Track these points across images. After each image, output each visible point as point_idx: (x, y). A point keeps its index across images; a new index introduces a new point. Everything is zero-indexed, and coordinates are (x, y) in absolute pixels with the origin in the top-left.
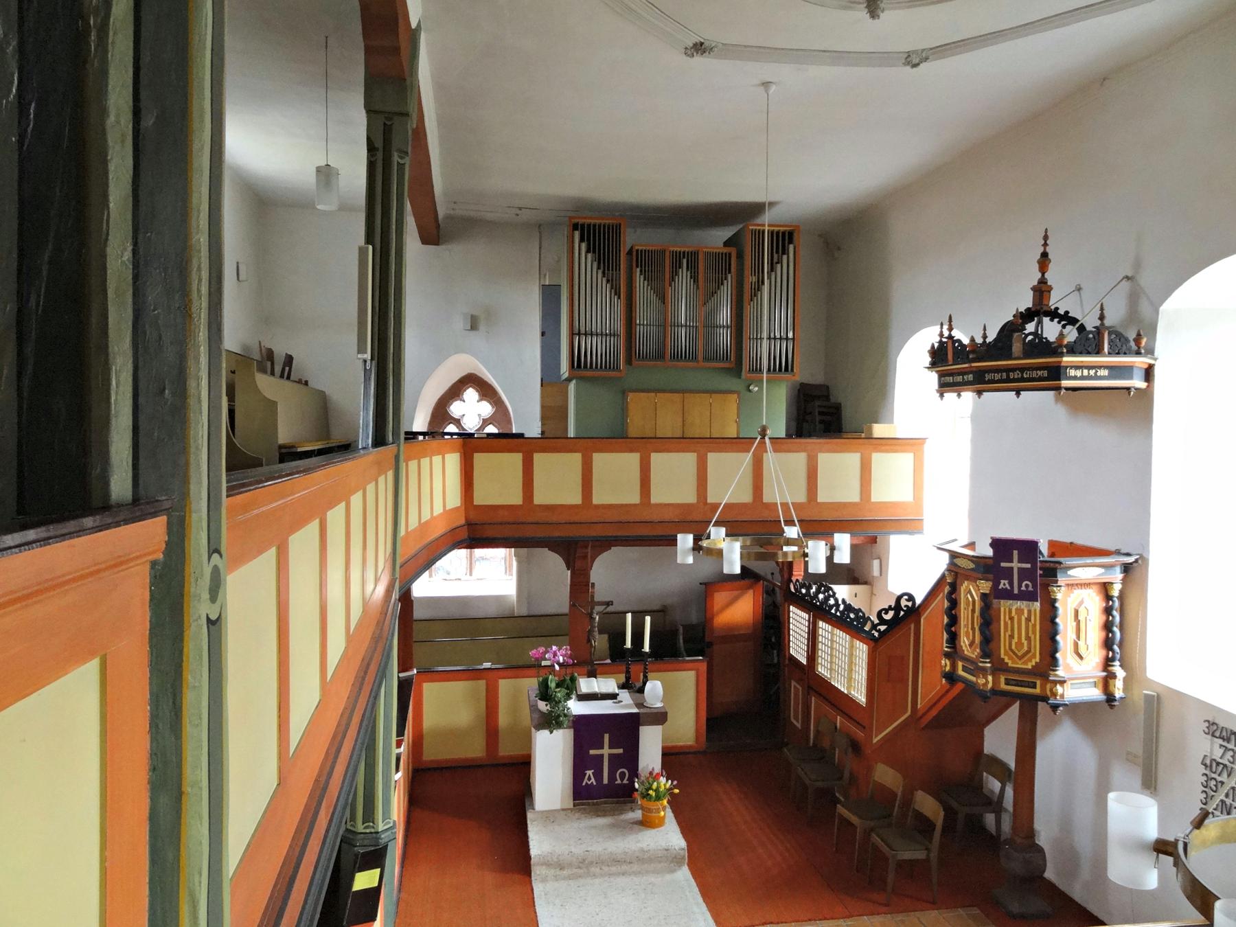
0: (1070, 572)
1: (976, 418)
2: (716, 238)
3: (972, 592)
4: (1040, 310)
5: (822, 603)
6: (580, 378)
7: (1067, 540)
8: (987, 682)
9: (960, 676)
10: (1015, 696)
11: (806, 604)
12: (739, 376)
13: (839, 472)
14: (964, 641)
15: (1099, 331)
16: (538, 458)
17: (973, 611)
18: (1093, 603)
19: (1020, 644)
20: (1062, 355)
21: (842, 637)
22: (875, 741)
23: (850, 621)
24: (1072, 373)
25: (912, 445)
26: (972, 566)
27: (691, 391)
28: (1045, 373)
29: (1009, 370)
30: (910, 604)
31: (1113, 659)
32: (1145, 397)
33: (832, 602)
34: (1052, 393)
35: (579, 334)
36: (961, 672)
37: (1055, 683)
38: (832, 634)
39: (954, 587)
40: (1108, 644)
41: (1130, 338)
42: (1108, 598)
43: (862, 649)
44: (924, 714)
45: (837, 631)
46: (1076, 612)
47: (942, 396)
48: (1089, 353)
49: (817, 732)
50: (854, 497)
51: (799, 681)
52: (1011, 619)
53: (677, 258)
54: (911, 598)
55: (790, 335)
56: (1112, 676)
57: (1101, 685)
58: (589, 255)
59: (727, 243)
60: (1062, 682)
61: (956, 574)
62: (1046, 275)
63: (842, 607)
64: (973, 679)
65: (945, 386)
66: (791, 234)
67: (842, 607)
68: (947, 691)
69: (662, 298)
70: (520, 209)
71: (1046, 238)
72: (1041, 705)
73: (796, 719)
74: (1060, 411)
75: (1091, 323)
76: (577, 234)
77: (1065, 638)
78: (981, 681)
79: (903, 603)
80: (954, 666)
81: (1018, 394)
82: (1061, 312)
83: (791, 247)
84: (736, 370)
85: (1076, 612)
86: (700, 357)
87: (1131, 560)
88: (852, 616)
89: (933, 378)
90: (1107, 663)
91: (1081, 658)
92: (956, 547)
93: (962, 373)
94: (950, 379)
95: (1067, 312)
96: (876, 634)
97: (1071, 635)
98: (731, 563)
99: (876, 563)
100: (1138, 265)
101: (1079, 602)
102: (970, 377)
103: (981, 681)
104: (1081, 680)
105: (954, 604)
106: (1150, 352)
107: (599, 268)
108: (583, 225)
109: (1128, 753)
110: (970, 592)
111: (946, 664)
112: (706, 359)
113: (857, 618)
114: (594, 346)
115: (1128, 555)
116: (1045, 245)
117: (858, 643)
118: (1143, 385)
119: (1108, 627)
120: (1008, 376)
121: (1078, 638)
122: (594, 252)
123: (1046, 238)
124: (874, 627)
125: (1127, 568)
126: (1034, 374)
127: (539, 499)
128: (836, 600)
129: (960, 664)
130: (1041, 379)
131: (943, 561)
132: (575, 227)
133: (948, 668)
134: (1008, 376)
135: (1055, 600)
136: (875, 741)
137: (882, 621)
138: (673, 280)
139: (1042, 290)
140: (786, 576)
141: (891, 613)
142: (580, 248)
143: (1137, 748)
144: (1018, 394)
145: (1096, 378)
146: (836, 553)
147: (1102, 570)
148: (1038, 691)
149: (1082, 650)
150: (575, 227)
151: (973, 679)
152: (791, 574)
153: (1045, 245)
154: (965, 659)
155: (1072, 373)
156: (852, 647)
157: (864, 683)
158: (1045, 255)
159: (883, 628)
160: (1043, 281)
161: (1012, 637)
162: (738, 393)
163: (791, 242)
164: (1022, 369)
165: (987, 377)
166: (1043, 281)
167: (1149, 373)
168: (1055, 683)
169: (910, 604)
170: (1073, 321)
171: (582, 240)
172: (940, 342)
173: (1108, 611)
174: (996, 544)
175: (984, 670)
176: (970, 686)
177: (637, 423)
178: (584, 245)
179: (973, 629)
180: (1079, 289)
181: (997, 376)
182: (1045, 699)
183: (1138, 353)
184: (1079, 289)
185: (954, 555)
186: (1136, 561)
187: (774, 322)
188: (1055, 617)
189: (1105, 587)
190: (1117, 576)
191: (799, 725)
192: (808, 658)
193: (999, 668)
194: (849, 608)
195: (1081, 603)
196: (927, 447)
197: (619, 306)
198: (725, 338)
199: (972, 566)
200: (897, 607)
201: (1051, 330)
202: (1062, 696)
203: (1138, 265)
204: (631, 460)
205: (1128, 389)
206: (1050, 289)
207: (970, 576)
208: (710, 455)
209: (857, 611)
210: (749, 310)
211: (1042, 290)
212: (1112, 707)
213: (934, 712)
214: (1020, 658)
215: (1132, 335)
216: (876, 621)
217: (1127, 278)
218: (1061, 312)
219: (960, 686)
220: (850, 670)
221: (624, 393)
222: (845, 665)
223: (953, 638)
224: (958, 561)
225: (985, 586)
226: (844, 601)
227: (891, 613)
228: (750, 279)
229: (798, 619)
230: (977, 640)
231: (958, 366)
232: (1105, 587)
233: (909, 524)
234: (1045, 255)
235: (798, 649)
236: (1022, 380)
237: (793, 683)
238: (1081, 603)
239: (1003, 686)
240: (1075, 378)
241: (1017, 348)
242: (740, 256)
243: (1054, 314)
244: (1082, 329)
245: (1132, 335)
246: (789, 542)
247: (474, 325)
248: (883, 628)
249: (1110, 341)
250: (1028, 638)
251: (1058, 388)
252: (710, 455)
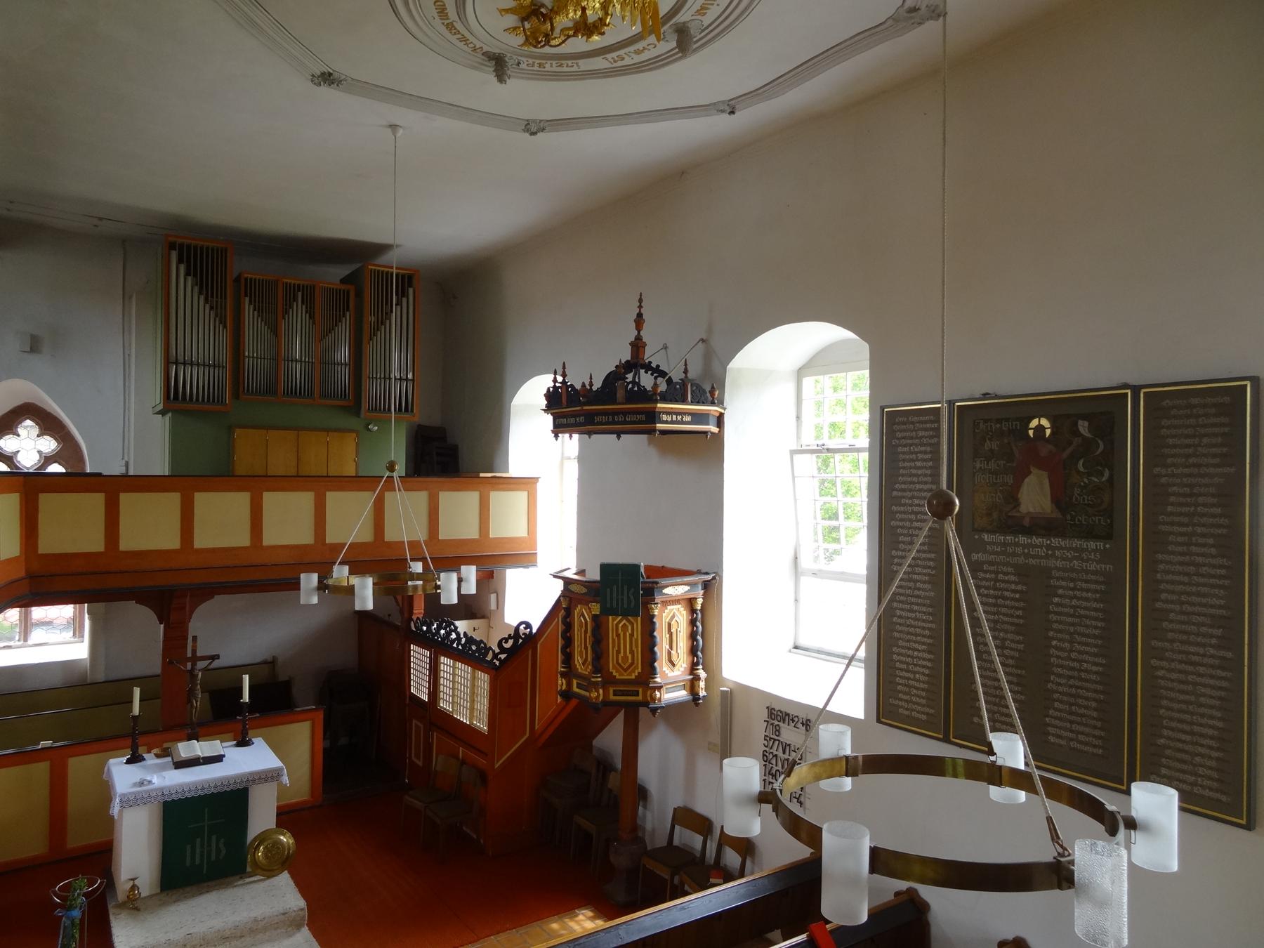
0: (666, 591)
1: (582, 459)
2: (334, 274)
3: (584, 615)
4: (636, 362)
5: (443, 639)
6: (176, 412)
7: (659, 564)
8: (597, 695)
9: (576, 693)
10: (619, 705)
11: (426, 641)
12: (357, 413)
13: (458, 512)
14: (578, 660)
15: (684, 383)
16: (125, 498)
17: (586, 632)
18: (679, 616)
19: (625, 657)
20: (656, 402)
21: (464, 669)
23: (472, 654)
24: (664, 417)
25: (527, 484)
26: (584, 590)
27: (303, 429)
28: (643, 417)
29: (615, 413)
31: (697, 664)
32: (718, 439)
33: (454, 636)
34: (645, 437)
35: (176, 363)
36: (575, 689)
37: (654, 689)
38: (454, 668)
39: (569, 612)
40: (693, 651)
41: (707, 388)
42: (693, 611)
43: (483, 679)
45: (459, 665)
46: (669, 625)
47: (556, 436)
48: (676, 401)
50: (472, 532)
52: (618, 635)
53: (292, 291)
54: (528, 626)
55: (410, 376)
56: (697, 678)
57: (688, 687)
58: (189, 279)
59: (343, 281)
60: (659, 688)
61: (571, 599)
63: (463, 641)
64: (587, 694)
65: (558, 429)
66: (410, 277)
67: (463, 641)
68: (564, 708)
69: (275, 331)
70: (101, 219)
71: (641, 301)
72: (642, 711)
73: (418, 757)
74: (652, 452)
75: (677, 376)
76: (174, 255)
77: (662, 649)
78: (594, 695)
80: (569, 684)
81: (619, 437)
82: (654, 365)
83: (411, 290)
84: (354, 407)
85: (669, 625)
86: (316, 395)
87: (709, 577)
88: (474, 648)
89: (549, 418)
90: (693, 668)
91: (673, 665)
92: (570, 574)
93: (575, 415)
94: (564, 421)
95: (658, 366)
97: (666, 646)
98: (364, 600)
99: (493, 597)
100: (710, 330)
101: (672, 619)
102: (582, 419)
103: (594, 695)
104: (674, 685)
105: (568, 626)
106: (721, 403)
107: (200, 293)
108: (181, 246)
109: (710, 743)
110: (583, 615)
111: (562, 683)
112: (324, 396)
113: (478, 650)
114: (194, 378)
115: (707, 574)
116: (640, 307)
117: (479, 674)
118: (715, 430)
119: (693, 636)
121: (671, 647)
122: (195, 275)
123: (641, 301)
124: (495, 656)
125: (706, 586)
126: (635, 418)
127: (128, 542)
128: (458, 634)
129: (575, 682)
130: (640, 422)
131: (559, 586)
132: (172, 246)
135: (653, 616)
137: (503, 650)
138: (287, 312)
139: (638, 346)
140: (406, 615)
141: (511, 642)
142: (177, 271)
143: (716, 738)
144: (619, 437)
145: (682, 422)
146: (463, 584)
147: (687, 588)
148: (640, 698)
149: (674, 658)
150: (172, 246)
151: (587, 694)
152: (411, 613)
153: (640, 307)
154: (580, 676)
155: (664, 417)
156: (474, 678)
157: (486, 712)
158: (640, 315)
159: (503, 656)
160: (638, 338)
161: (618, 652)
162: (357, 432)
163: (410, 285)
164: (625, 413)
165: (596, 419)
166: (638, 338)
167: (720, 421)
168: (654, 689)
170: (663, 374)
171: (180, 261)
172: (554, 387)
173: (693, 622)
174: (605, 568)
175: (596, 685)
176: (584, 701)
177: (245, 459)
178: (182, 268)
179: (586, 648)
180: (665, 347)
181: (604, 419)
182: (645, 704)
183: (713, 403)
184: (665, 347)
185: (568, 582)
186: (714, 578)
187: (396, 362)
188: (654, 630)
189: (691, 602)
190: (700, 592)
191: (420, 764)
193: (609, 681)
194: (470, 640)
195: (673, 617)
196: (540, 486)
197: (225, 336)
198: (343, 376)
199: (584, 590)
201: (646, 380)
202: (660, 700)
203: (710, 330)
204: (239, 502)
205: (705, 433)
206: (644, 345)
207: (584, 600)
208: (329, 494)
209: (478, 643)
210: (370, 349)
211: (638, 346)
212: (697, 705)
214: (625, 670)
215: (708, 388)
216: (497, 650)
217: (703, 340)
218: (654, 365)
219: (574, 702)
220: (472, 701)
221: (230, 429)
222: (464, 695)
223: (568, 659)
224: (573, 588)
225: (596, 608)
226: (465, 634)
227: (511, 642)
228: (370, 319)
229: (419, 657)
230: (589, 659)
231: (569, 409)
232: (691, 602)
233: (525, 558)
234: (640, 315)
235: (419, 688)
236: (625, 422)
238: (673, 617)
239: (612, 697)
240: (666, 422)
241: (620, 394)
242: (359, 294)
243: (648, 367)
244: (669, 381)
245: (708, 388)
246: (414, 577)
247: (34, 346)
248: (503, 656)
249: (693, 392)
250: (632, 652)
251: (654, 430)
252: (329, 494)
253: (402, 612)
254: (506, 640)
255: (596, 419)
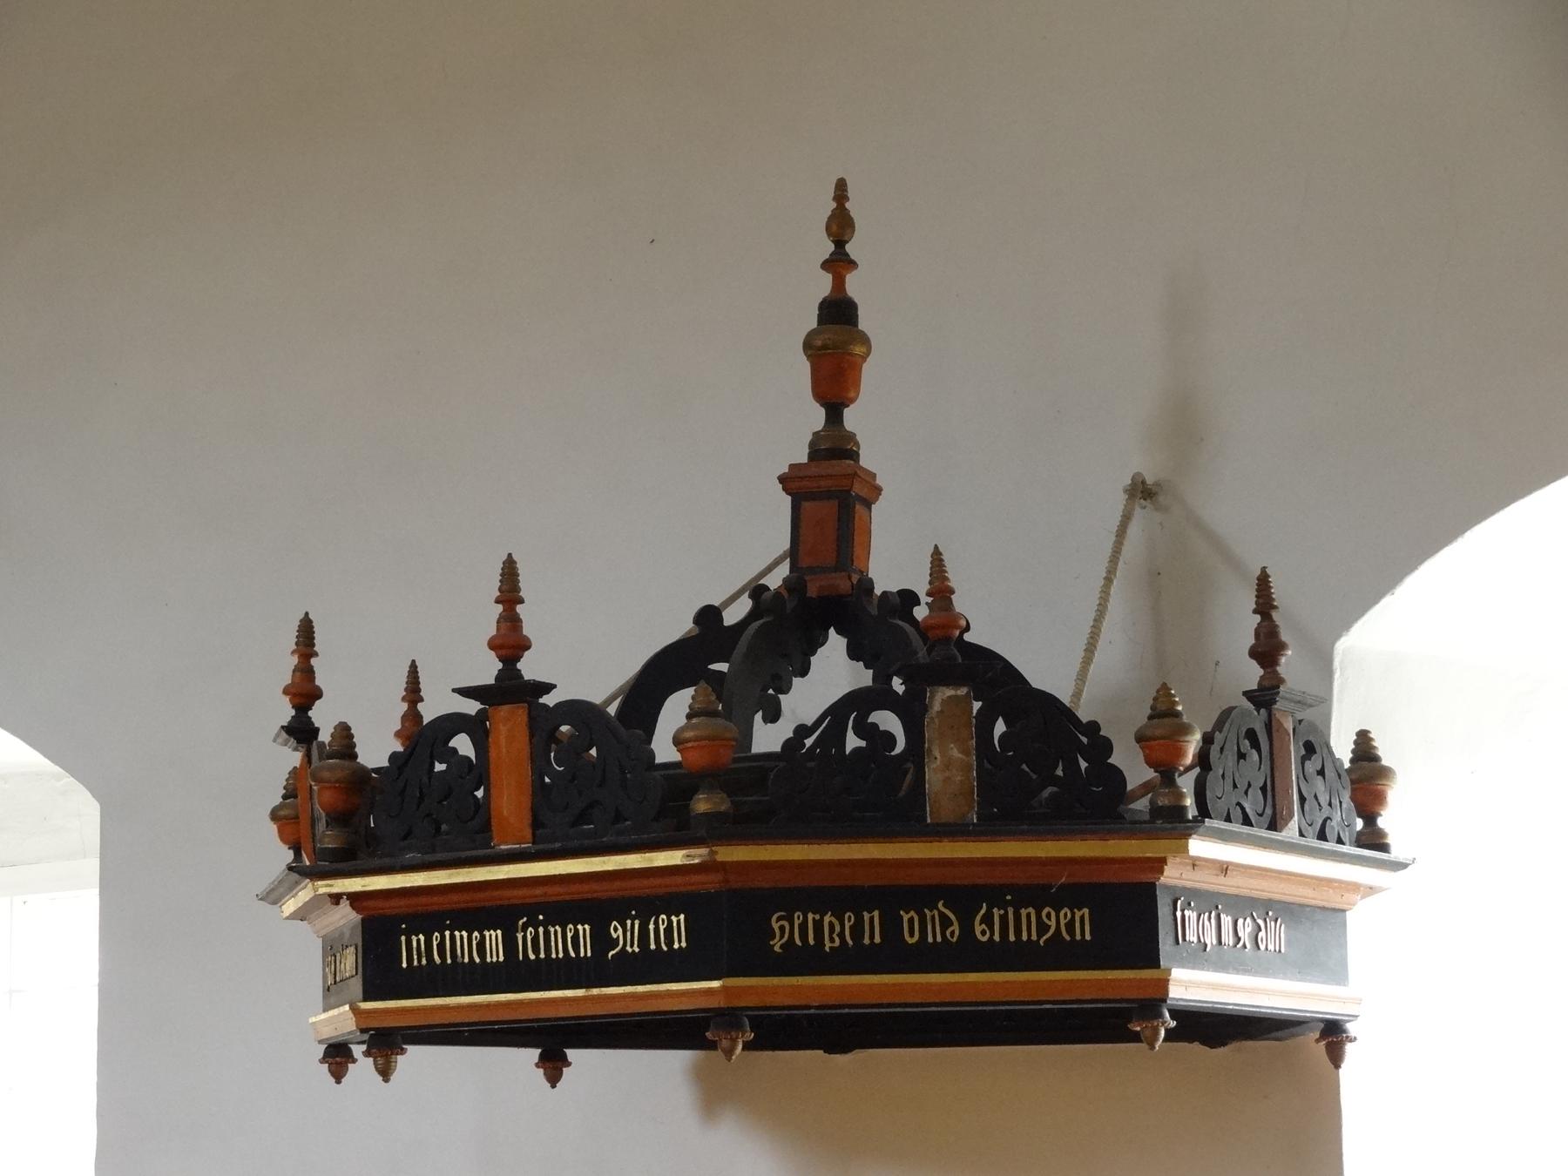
28: (1081, 923)
29: (895, 894)
62: (852, 418)
71: (840, 226)
81: (553, 1065)
116: (839, 263)
120: (892, 926)
123: (840, 226)
126: (1028, 925)
134: (892, 926)
139: (830, 490)
144: (553, 1065)
153: (839, 263)
158: (838, 312)
160: (834, 447)
164: (965, 894)
165: (782, 931)
166: (834, 447)
181: (834, 930)
211: (830, 490)
234: (838, 312)
236: (967, 955)
255: (782, 931)
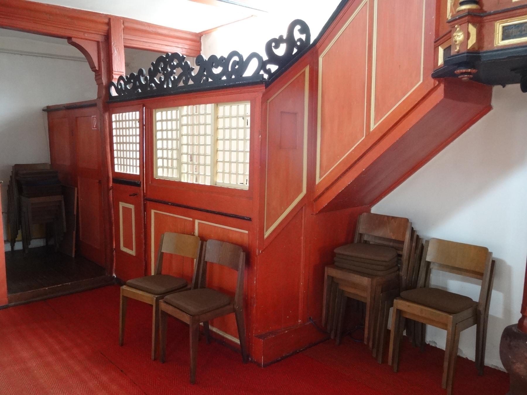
22: (267, 234)
30: (303, 37)
44: (327, 189)
49: (161, 256)
51: (132, 198)
54: (305, 29)
73: (128, 245)
79: (297, 35)
96: (266, 76)
124: (263, 65)
133: (472, 41)
136: (267, 234)
137: (273, 58)
140: (104, 80)
159: (273, 68)
169: (303, 37)
191: (133, 253)
192: (141, 167)
200: (290, 41)
213: (348, 180)
216: (265, 58)
229: (125, 124)
235: (126, 162)
237: (122, 205)
248: (273, 68)
253: (98, 73)
254: (278, 42)
